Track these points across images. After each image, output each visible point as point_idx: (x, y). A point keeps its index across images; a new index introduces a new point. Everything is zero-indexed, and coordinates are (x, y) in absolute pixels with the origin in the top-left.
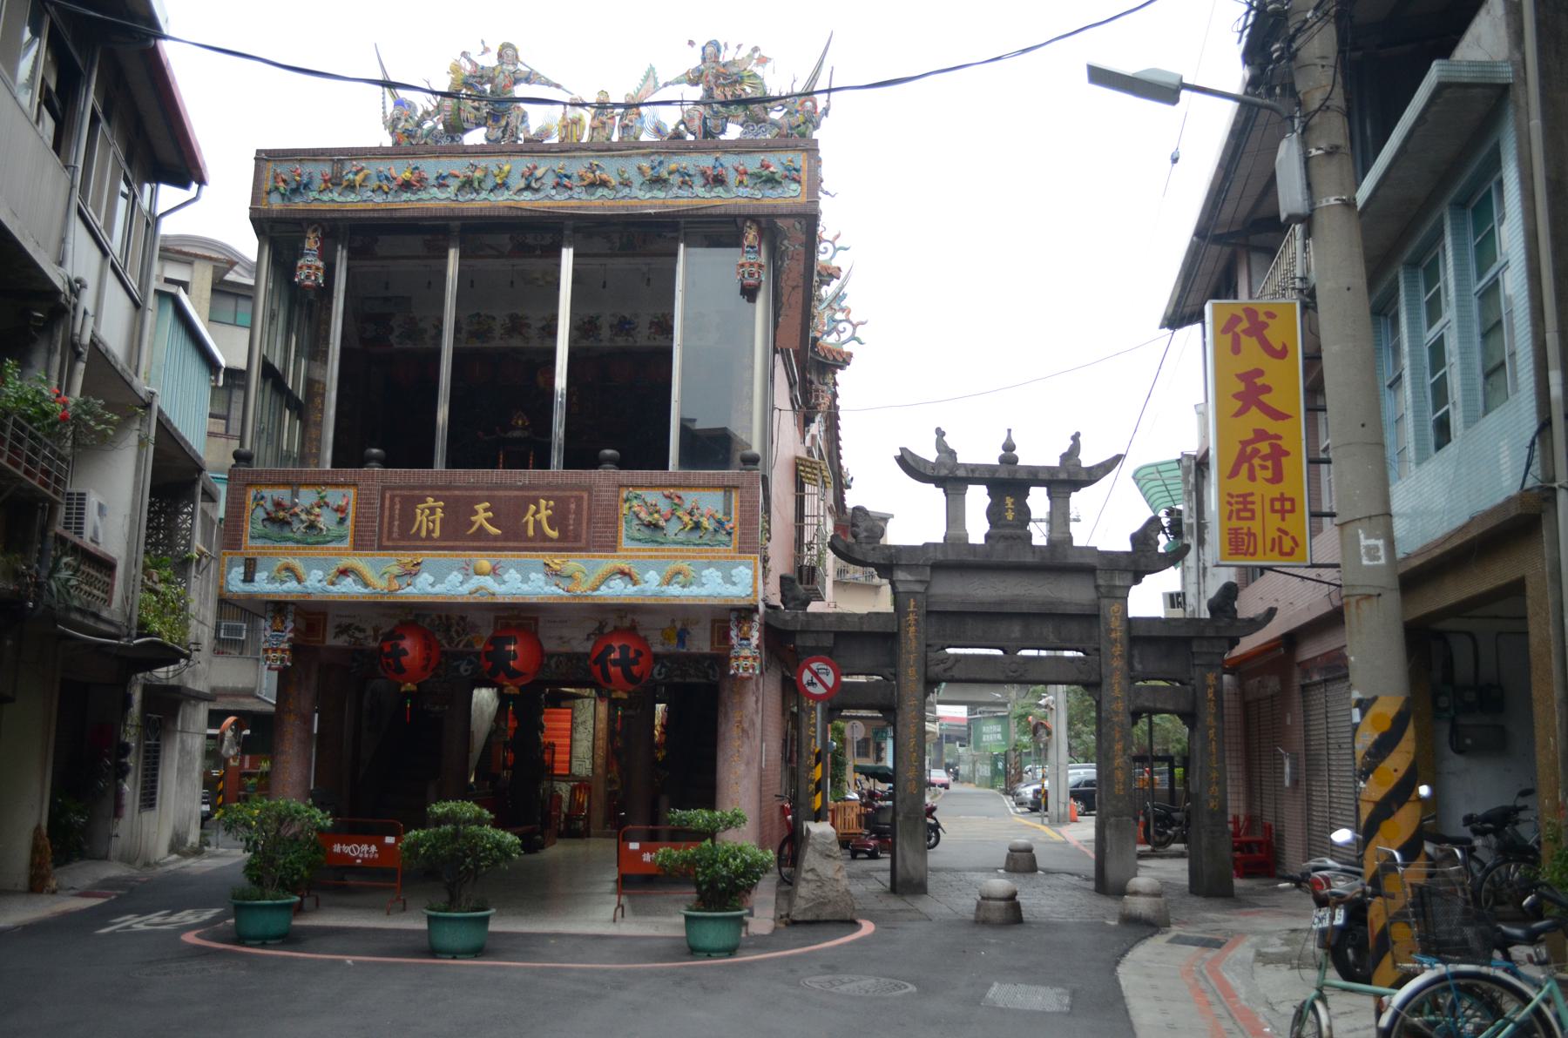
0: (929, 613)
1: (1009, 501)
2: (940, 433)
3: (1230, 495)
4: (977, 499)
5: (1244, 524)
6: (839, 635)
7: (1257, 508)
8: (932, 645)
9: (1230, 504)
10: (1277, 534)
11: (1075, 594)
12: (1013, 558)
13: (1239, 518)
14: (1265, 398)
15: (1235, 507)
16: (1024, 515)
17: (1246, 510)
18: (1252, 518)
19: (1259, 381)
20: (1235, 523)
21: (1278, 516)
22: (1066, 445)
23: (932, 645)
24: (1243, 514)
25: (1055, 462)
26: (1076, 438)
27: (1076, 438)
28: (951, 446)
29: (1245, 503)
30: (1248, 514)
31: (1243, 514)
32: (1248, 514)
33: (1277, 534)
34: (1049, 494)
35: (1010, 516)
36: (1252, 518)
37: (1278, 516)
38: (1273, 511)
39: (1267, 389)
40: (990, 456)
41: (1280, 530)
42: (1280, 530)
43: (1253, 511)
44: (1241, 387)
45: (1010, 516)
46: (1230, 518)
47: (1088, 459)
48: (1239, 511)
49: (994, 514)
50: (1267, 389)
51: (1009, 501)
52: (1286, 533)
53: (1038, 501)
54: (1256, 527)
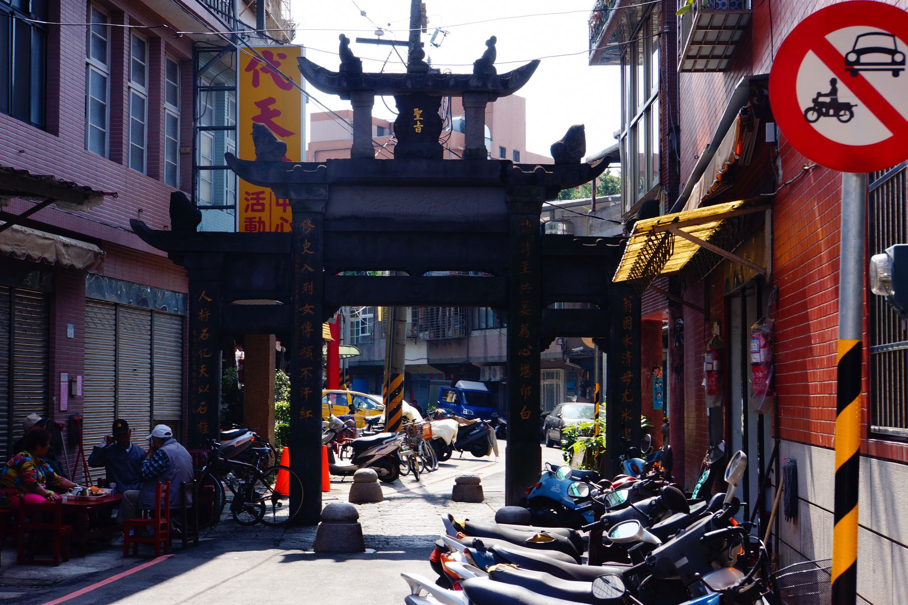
3: (247, 193)
5: (257, 215)
7: (266, 202)
9: (247, 199)
10: (280, 222)
13: (253, 210)
14: (275, 120)
15: (251, 202)
17: (258, 204)
18: (263, 210)
19: (272, 107)
20: (250, 214)
21: (281, 208)
24: (256, 207)
29: (258, 199)
30: (260, 207)
31: (256, 207)
32: (260, 207)
33: (280, 222)
36: (263, 210)
37: (281, 208)
38: (278, 204)
39: (277, 113)
41: (282, 218)
42: (282, 218)
43: (263, 205)
44: (258, 112)
46: (246, 211)
48: (253, 205)
50: (277, 113)
52: (287, 221)
54: (265, 216)
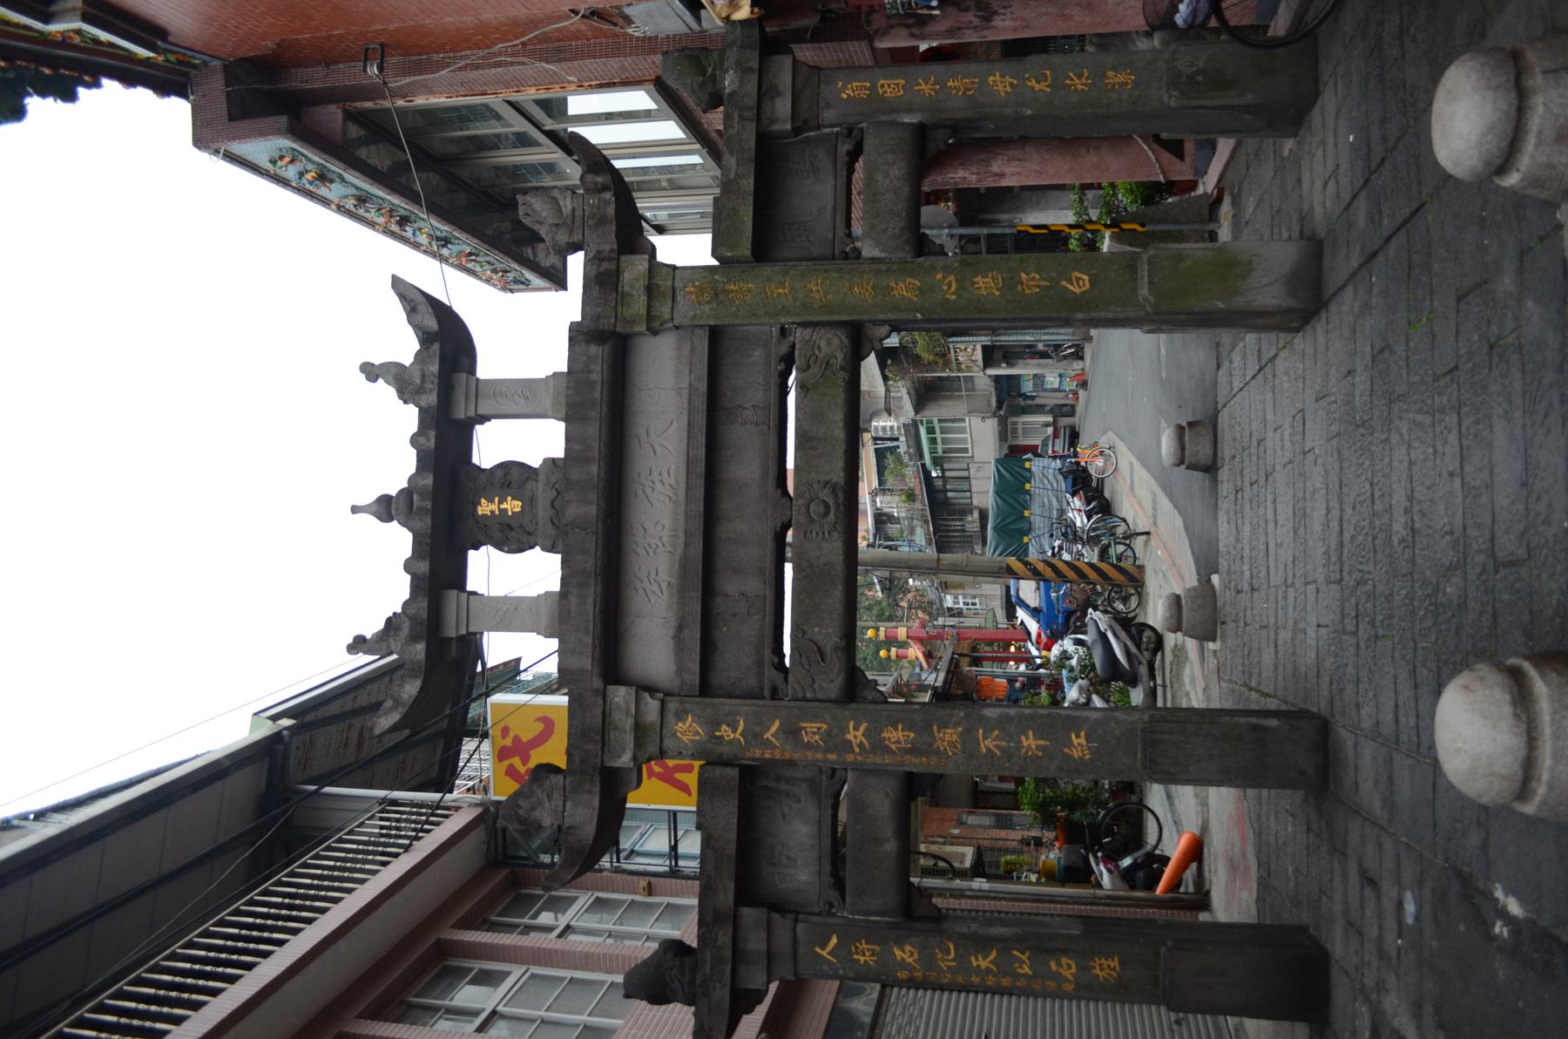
0: (706, 688)
1: (485, 508)
2: (358, 645)
4: (493, 572)
6: (748, 892)
8: (772, 686)
11: (665, 377)
12: (585, 509)
16: (511, 475)
22: (385, 391)
23: (772, 686)
25: (408, 418)
26: (371, 372)
27: (371, 372)
28: (381, 626)
34: (483, 419)
35: (513, 506)
40: (398, 540)
45: (513, 506)
47: (403, 346)
49: (512, 538)
51: (485, 508)
53: (492, 444)
